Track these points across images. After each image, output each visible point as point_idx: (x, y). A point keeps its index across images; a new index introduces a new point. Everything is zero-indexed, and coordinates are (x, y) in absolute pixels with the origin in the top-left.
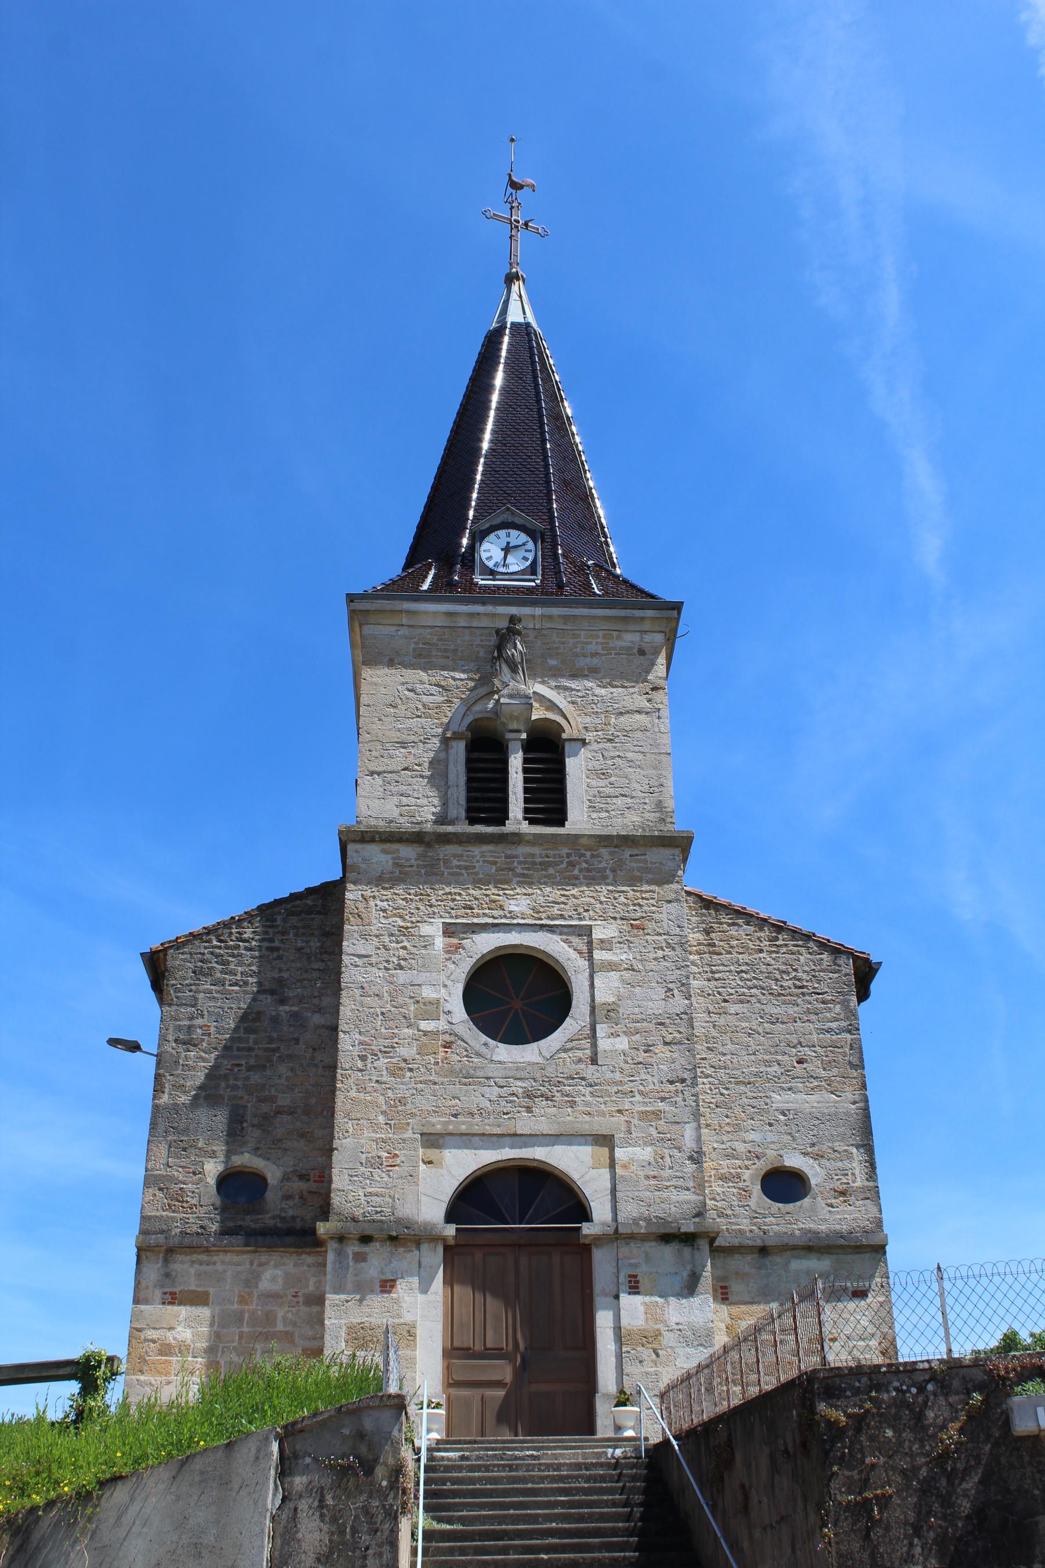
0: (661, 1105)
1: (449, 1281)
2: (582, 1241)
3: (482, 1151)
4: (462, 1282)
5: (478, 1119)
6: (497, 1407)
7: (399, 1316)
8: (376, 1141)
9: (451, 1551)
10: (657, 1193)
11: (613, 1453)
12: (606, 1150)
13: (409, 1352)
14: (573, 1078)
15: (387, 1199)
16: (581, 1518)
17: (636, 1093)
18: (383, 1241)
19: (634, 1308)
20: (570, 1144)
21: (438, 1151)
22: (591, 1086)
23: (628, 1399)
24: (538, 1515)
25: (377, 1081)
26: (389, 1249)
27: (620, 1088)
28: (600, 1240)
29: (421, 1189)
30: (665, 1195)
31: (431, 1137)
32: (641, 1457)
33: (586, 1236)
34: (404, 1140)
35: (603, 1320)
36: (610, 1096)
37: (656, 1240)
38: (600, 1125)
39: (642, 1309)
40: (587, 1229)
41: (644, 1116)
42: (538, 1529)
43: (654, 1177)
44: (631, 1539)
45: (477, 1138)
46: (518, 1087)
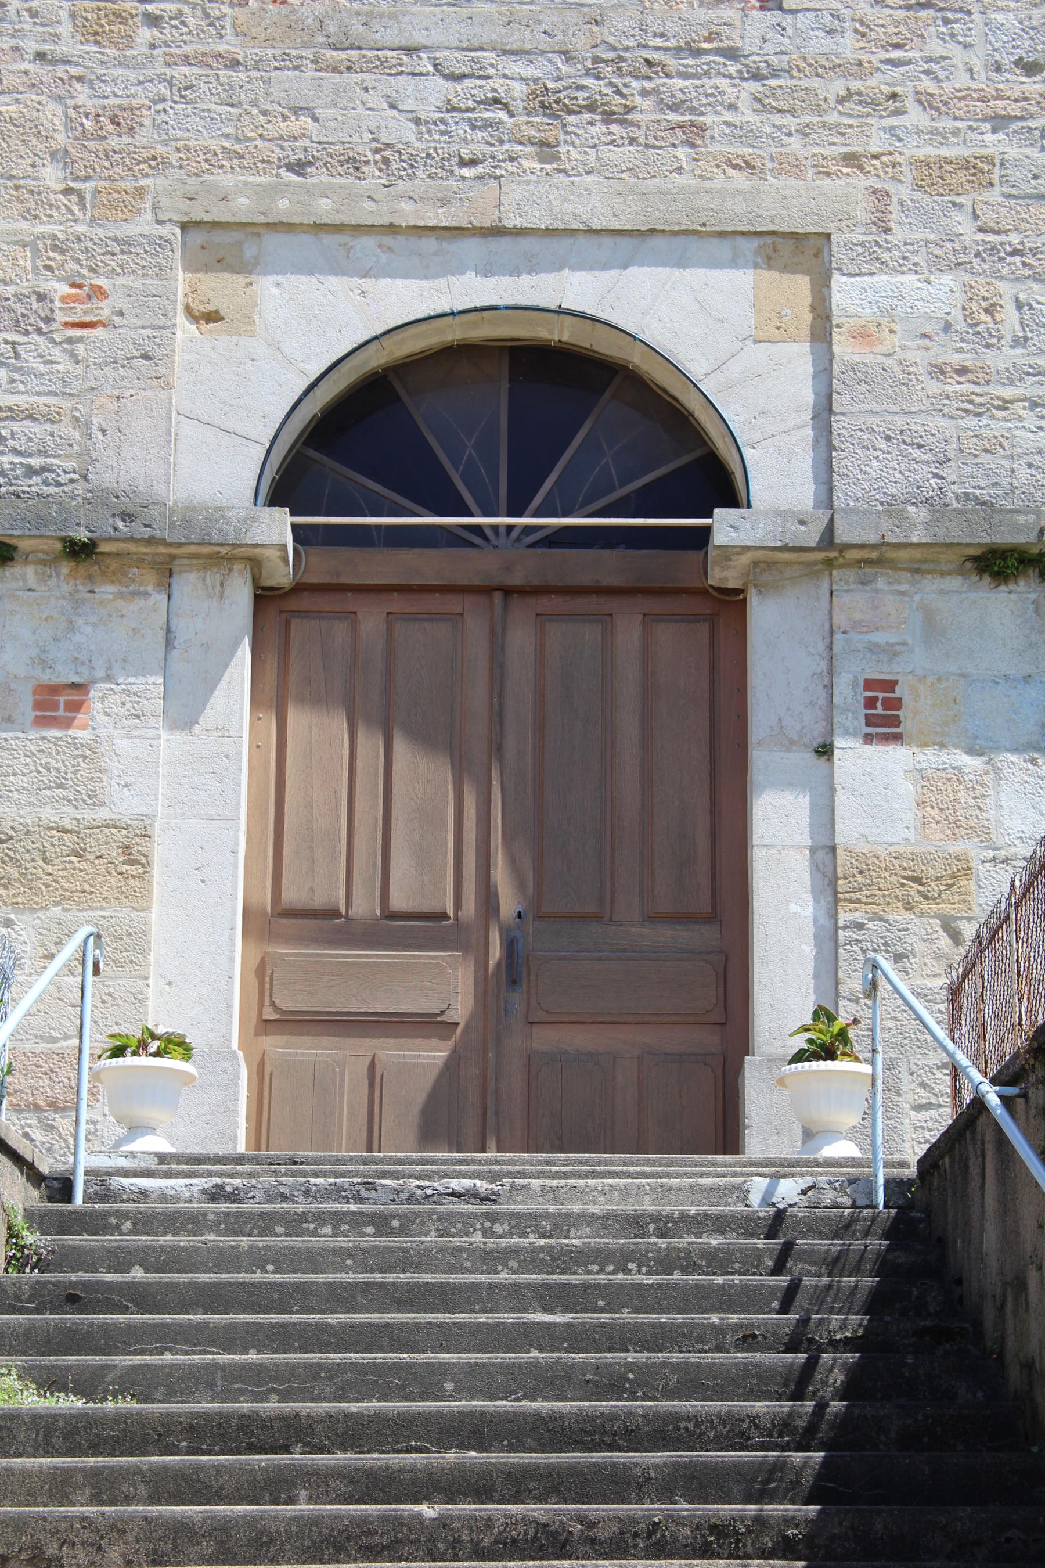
0: (993, 142)
1: (273, 695)
2: (719, 576)
3: (385, 283)
4: (316, 699)
5: (373, 178)
6: (420, 1098)
7: (94, 800)
8: (29, 244)
9: (60, 1487)
10: (971, 422)
11: (769, 1192)
12: (801, 284)
13: (124, 913)
14: (698, 53)
15: (66, 429)
16: (613, 1384)
17: (910, 104)
18: (49, 561)
19: (881, 789)
20: (682, 263)
21: (240, 280)
22: (757, 77)
23: (842, 1035)
24: (442, 1370)
25: (40, 56)
26: (66, 588)
27: (855, 85)
28: (773, 565)
29: (179, 399)
30: (996, 427)
31: (219, 237)
32: (875, 1207)
33: (728, 552)
34: (125, 244)
35: (778, 823)
36: (818, 110)
37: (961, 571)
38: (786, 202)
39: (907, 789)
40: (726, 527)
41: (933, 175)
42: (425, 1418)
43: (962, 371)
44: (797, 1457)
45: (369, 242)
46: (513, 78)
